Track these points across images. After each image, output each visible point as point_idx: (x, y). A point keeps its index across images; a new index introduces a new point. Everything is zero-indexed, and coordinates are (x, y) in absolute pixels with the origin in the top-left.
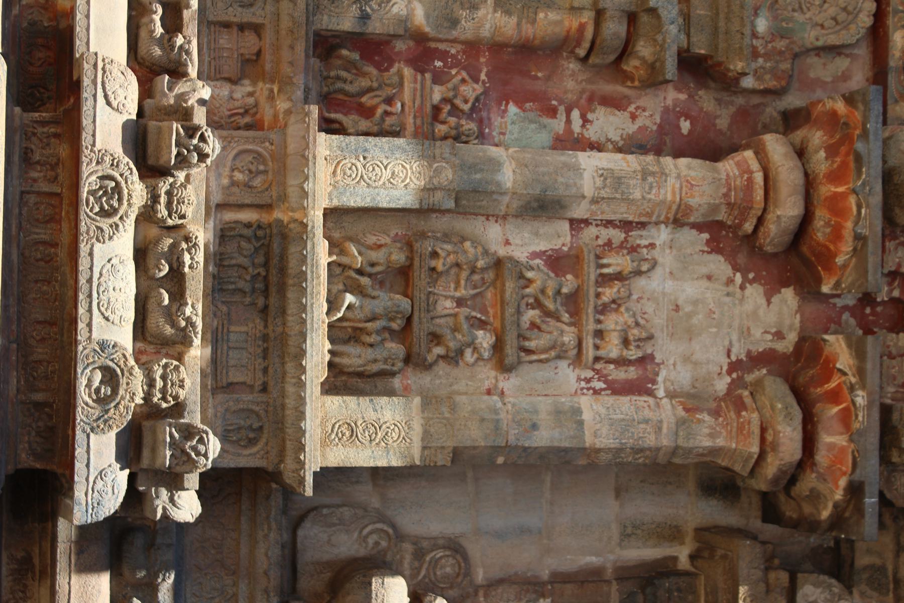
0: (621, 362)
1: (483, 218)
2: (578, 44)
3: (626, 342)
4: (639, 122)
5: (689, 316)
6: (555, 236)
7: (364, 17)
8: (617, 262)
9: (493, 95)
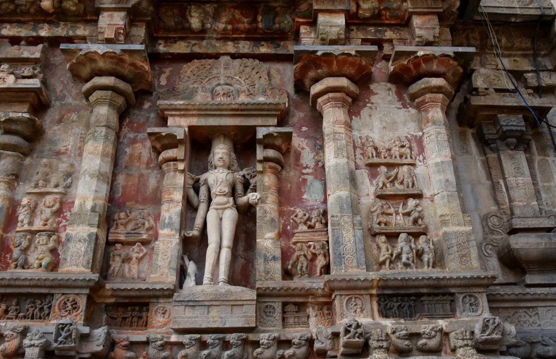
0: (410, 148)
2: (277, 169)
3: (403, 146)
5: (387, 123)
6: (363, 175)
7: (274, 258)
8: (370, 151)
9: (300, 204)
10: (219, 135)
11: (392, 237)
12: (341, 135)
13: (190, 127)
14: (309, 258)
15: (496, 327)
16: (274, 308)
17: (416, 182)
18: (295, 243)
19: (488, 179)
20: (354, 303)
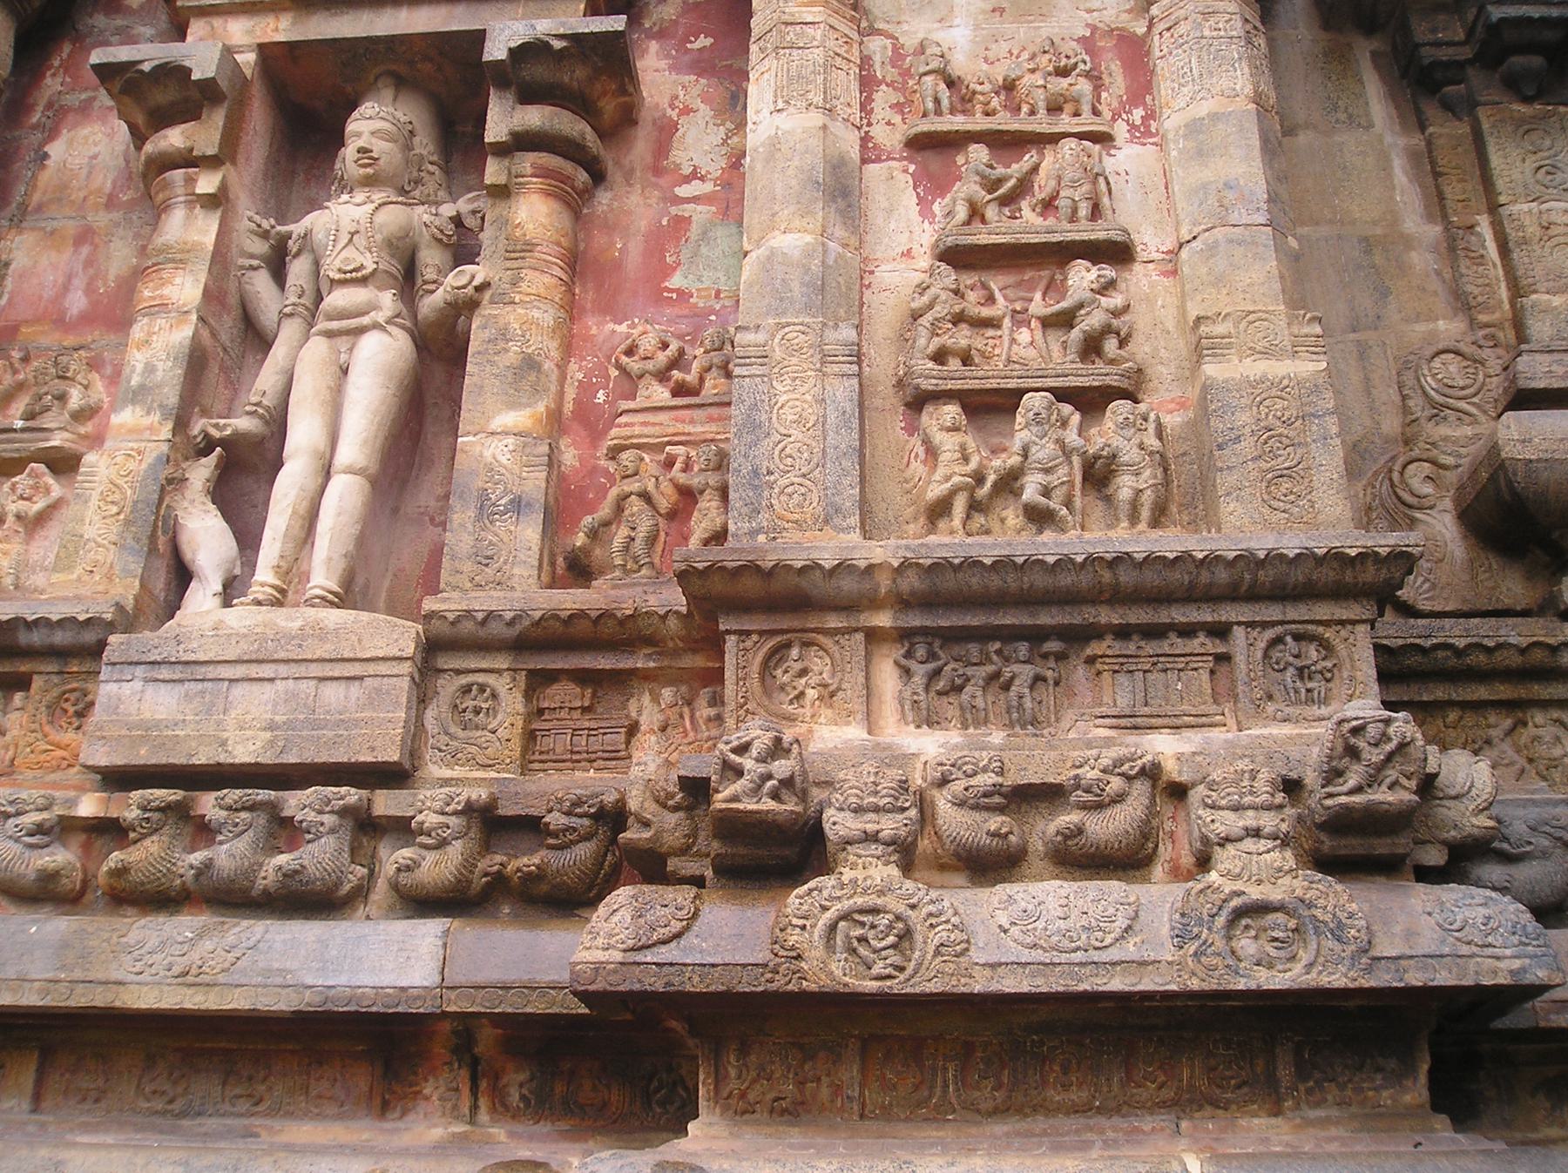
0: (1094, 77)
1: (867, 293)
3: (1063, 72)
4: (698, 104)
7: (518, 506)
10: (376, 79)
11: (990, 407)
12: (809, 30)
13: (264, 49)
14: (664, 505)
15: (1390, 757)
16: (494, 696)
17: (1105, 200)
18: (614, 452)
19: (1430, 218)
20: (798, 666)
